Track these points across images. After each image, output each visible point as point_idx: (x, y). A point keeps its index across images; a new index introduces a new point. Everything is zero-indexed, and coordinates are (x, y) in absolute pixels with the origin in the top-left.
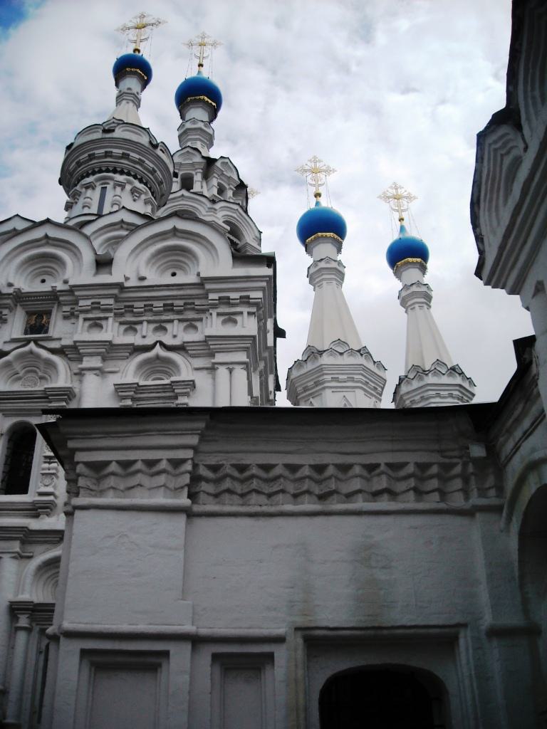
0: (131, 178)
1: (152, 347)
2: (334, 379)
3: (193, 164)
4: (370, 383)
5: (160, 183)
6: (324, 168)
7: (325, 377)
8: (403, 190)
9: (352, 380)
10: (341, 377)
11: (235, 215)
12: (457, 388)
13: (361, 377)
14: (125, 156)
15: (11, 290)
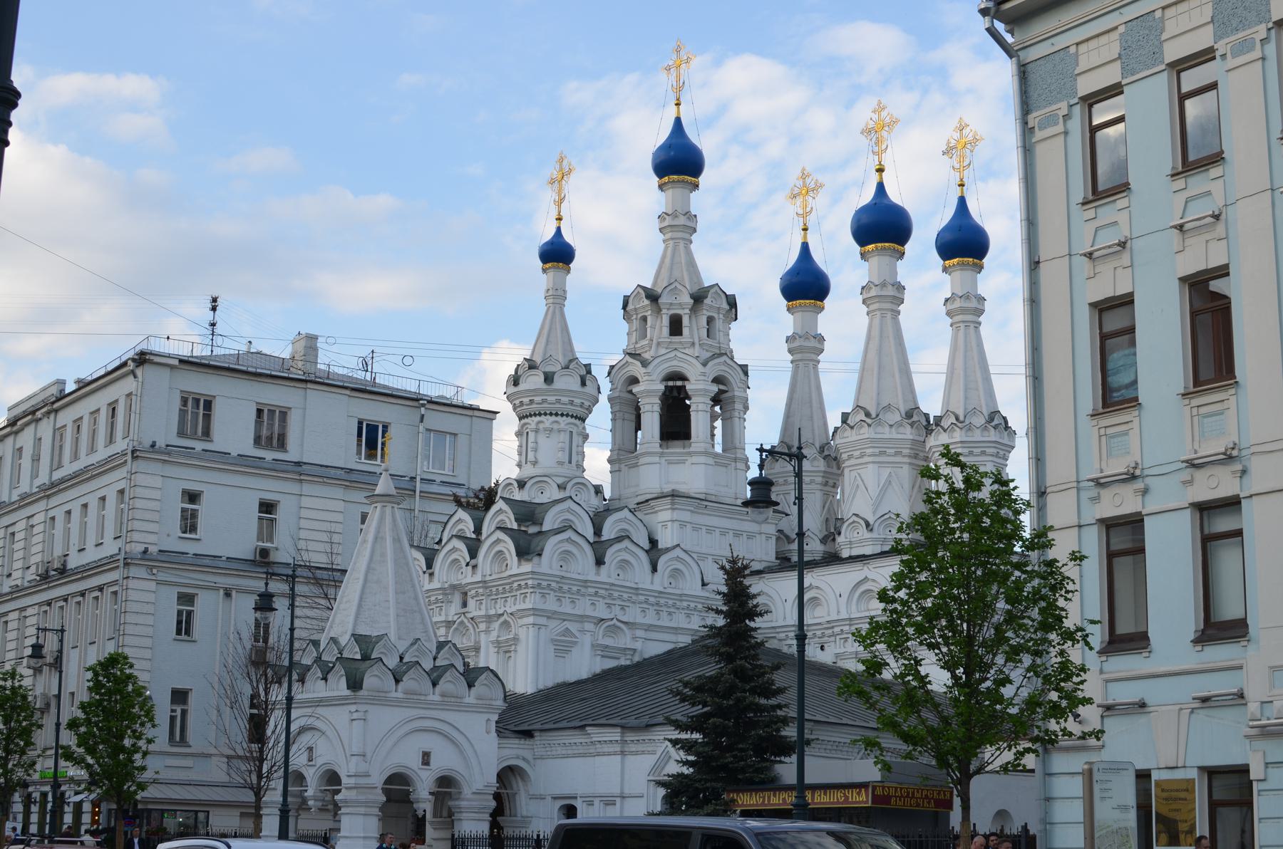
0: (543, 418)
1: (502, 615)
2: (850, 457)
3: (643, 307)
4: (888, 451)
5: (571, 403)
6: (888, 120)
7: (843, 455)
8: (968, 129)
9: (862, 456)
10: (857, 453)
11: (675, 363)
12: (959, 445)
13: (871, 450)
14: (532, 402)
15: (446, 586)
